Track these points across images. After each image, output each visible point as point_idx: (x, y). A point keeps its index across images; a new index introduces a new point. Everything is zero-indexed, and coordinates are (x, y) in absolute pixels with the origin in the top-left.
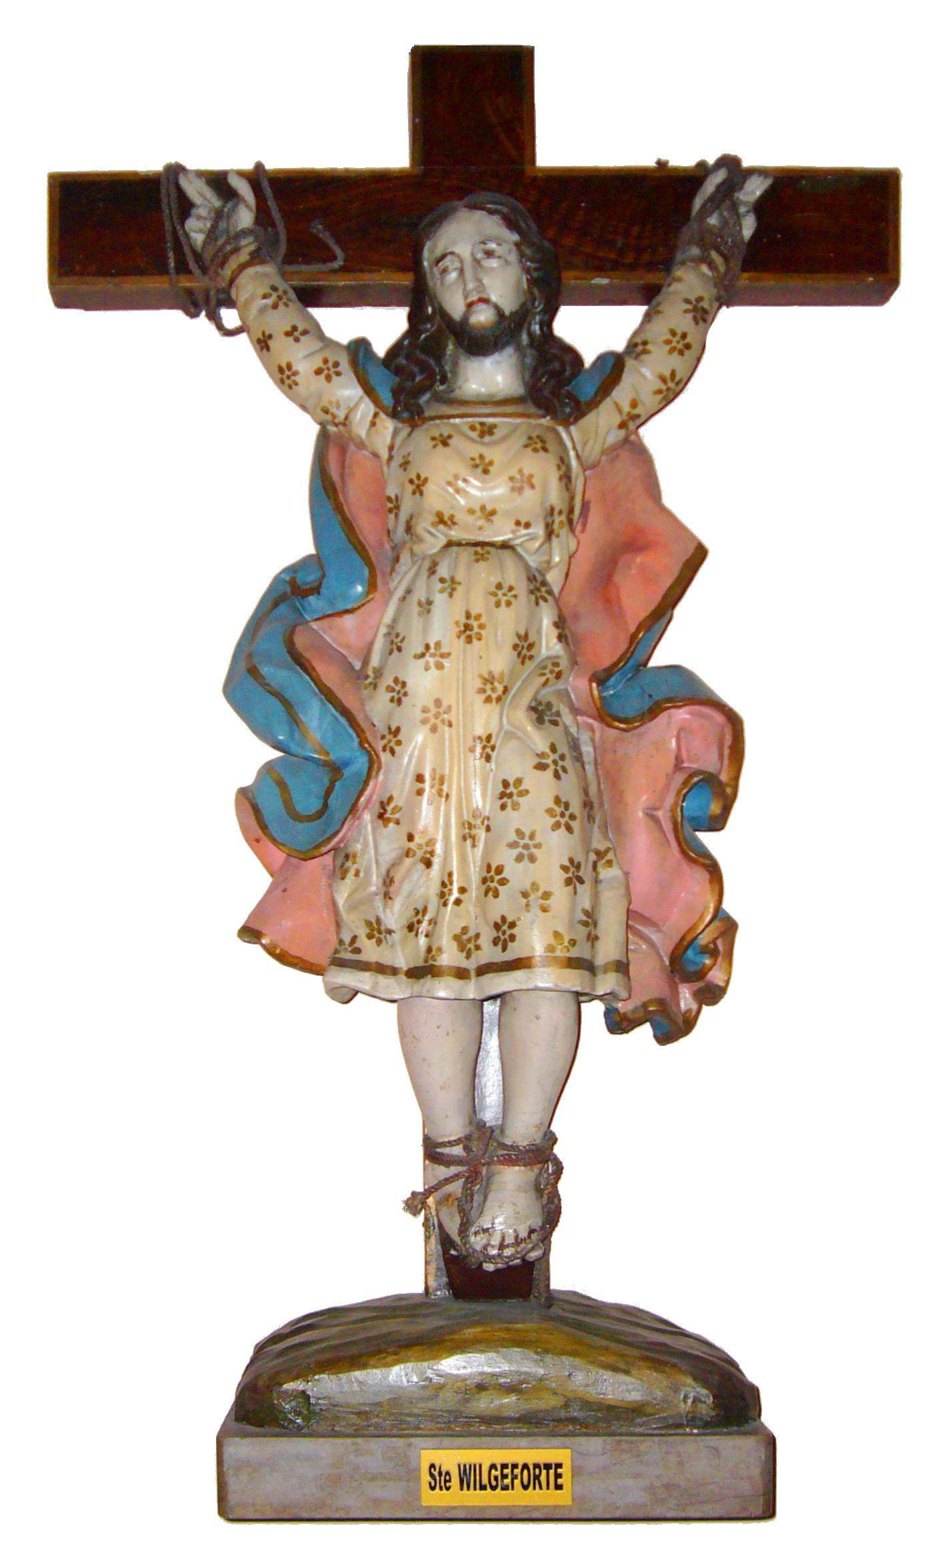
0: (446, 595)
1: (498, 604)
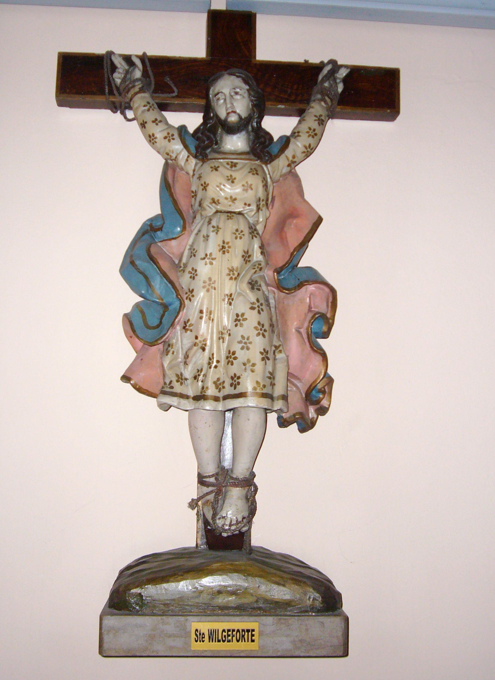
0: (215, 233)
1: (236, 238)
